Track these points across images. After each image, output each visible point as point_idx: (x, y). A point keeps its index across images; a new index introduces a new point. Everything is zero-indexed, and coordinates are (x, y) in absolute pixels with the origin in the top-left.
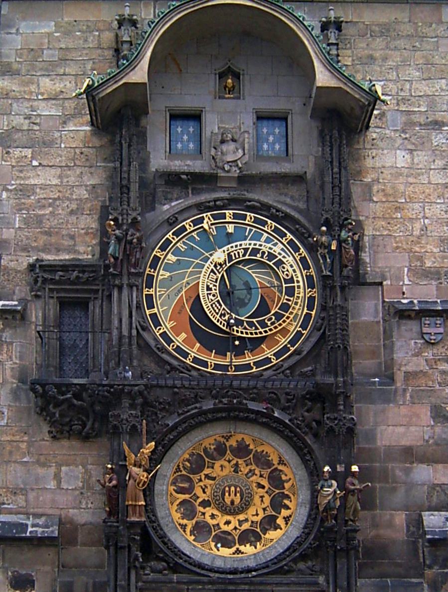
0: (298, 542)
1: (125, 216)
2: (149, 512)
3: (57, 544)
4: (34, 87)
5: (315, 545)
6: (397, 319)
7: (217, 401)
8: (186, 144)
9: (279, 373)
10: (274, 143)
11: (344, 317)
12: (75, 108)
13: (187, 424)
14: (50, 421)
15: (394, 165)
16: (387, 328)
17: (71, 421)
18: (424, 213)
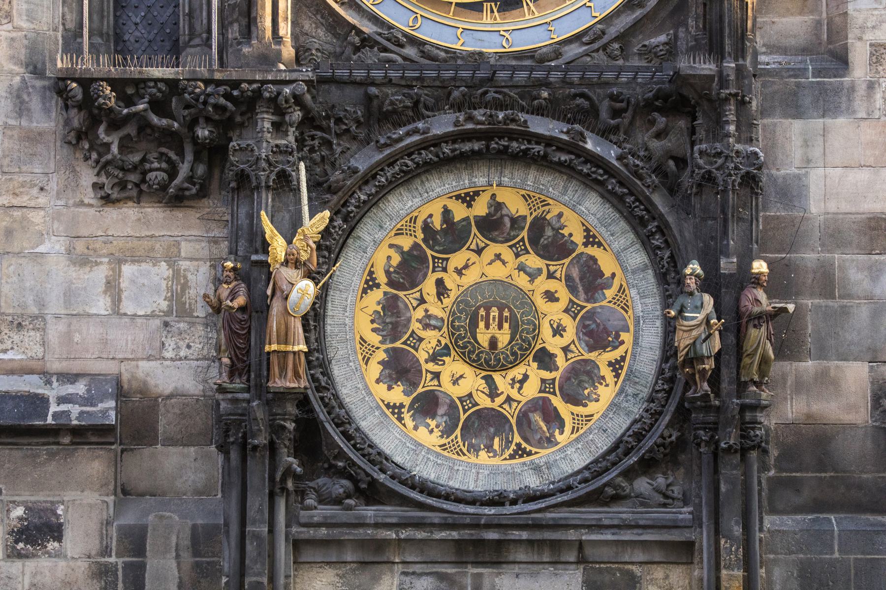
2: (315, 367)
3: (113, 440)
5: (673, 438)
9: (597, 50)
13: (397, 168)
14: (97, 162)
17: (144, 160)
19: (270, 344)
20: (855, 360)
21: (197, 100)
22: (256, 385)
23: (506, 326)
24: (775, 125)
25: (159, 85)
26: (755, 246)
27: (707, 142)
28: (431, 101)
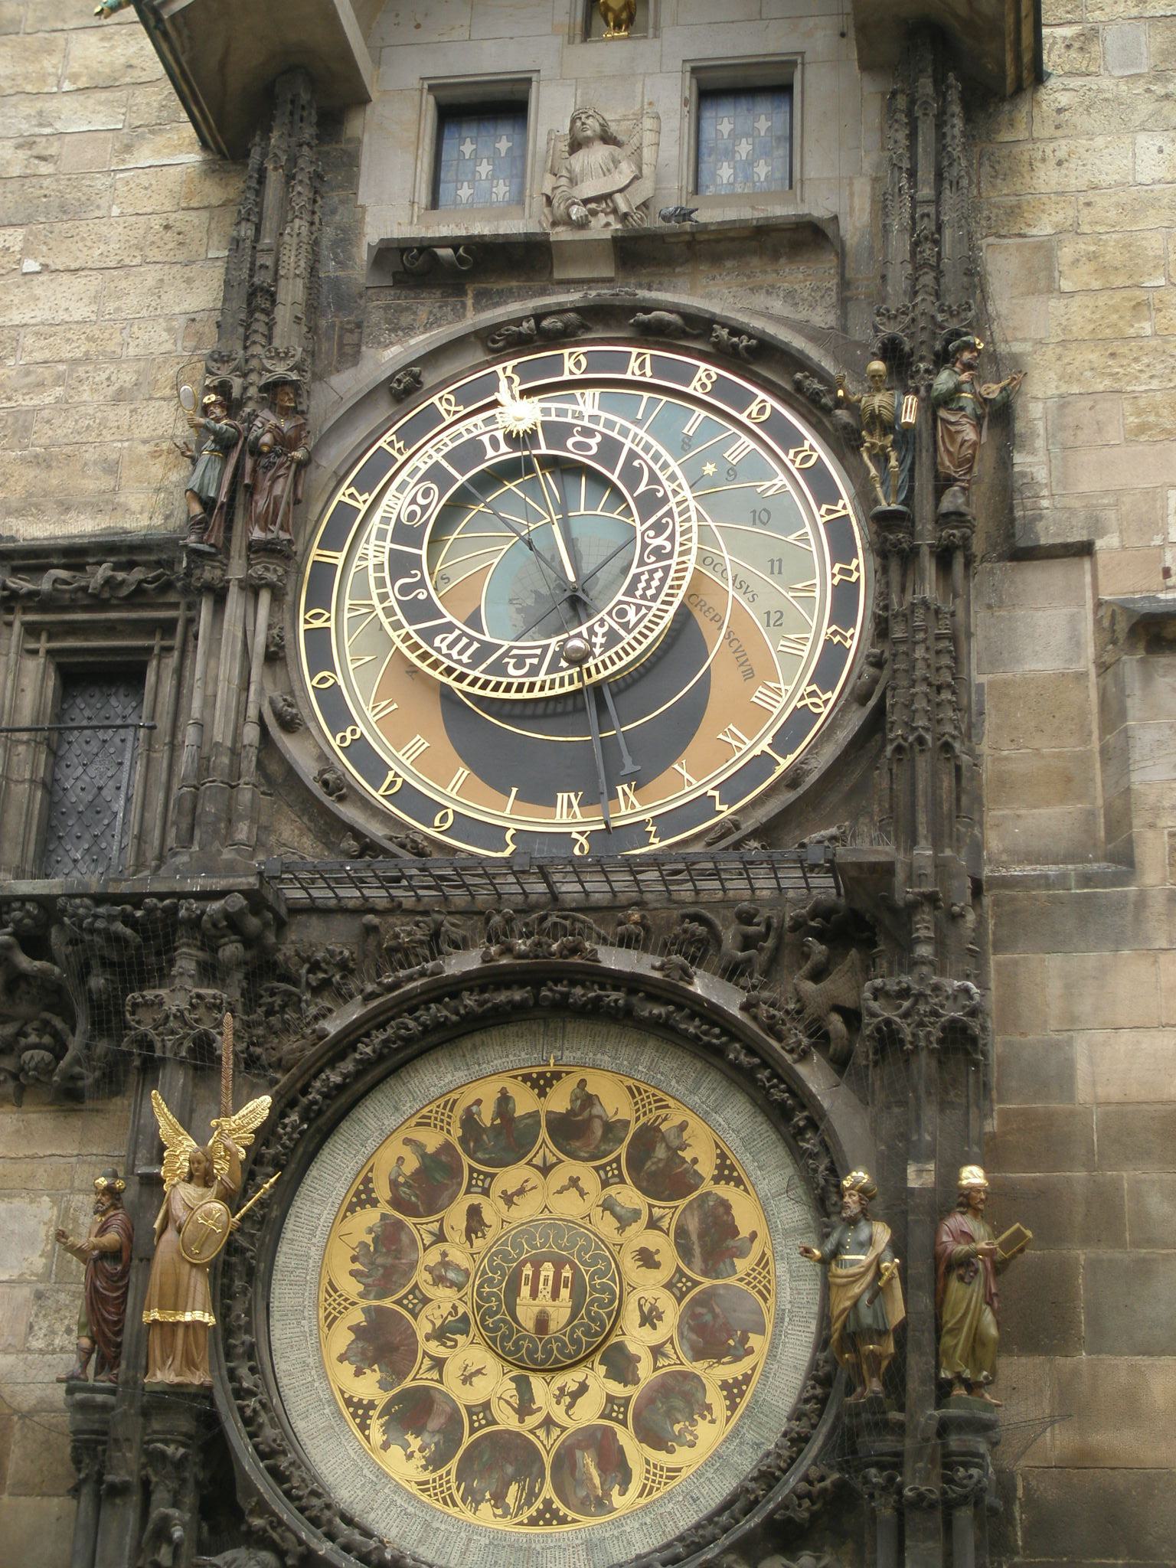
1: (253, 377)
5: (827, 1483)
6: (1141, 654)
7: (493, 949)
8: (486, 185)
15: (1130, 178)
20: (1163, 1352)
21: (80, 927)
23: (565, 1293)
24: (1016, 963)
28: (458, 934)
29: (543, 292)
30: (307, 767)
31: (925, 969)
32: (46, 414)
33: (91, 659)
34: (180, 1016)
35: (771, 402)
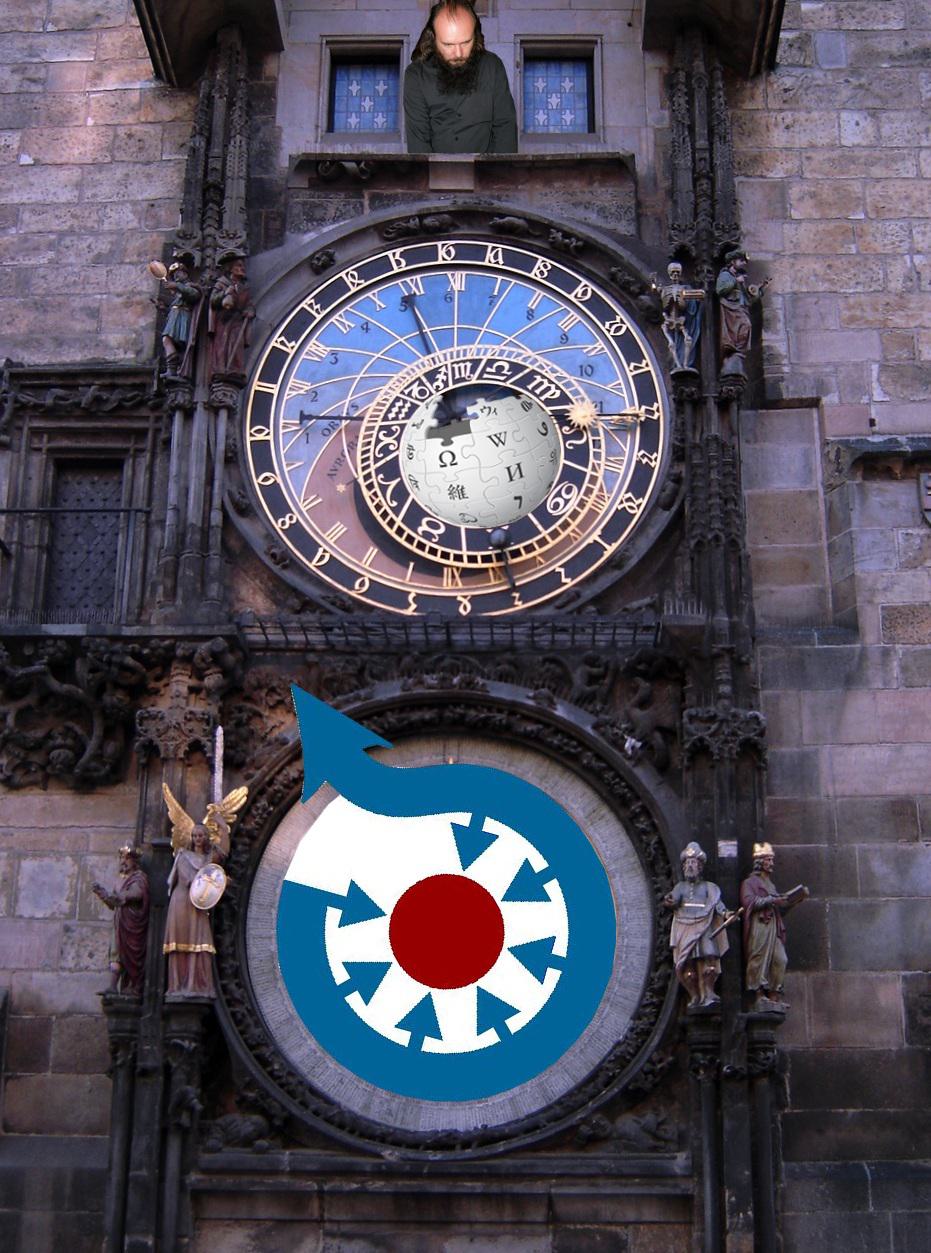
0: (620, 1057)
1: (209, 251)
4: (40, 9)
6: (859, 480)
7: (411, 681)
10: (561, 110)
11: (729, 469)
12: (124, 47)
16: (837, 504)
17: (49, 736)
18: (912, 243)
19: (168, 943)
21: (101, 660)
22: (150, 995)
24: (778, 697)
25: (59, 643)
26: (760, 829)
27: (699, 704)
29: (420, 198)
30: (260, 546)
31: (726, 702)
32: (41, 271)
33: (81, 456)
34: (178, 727)
35: (591, 287)
